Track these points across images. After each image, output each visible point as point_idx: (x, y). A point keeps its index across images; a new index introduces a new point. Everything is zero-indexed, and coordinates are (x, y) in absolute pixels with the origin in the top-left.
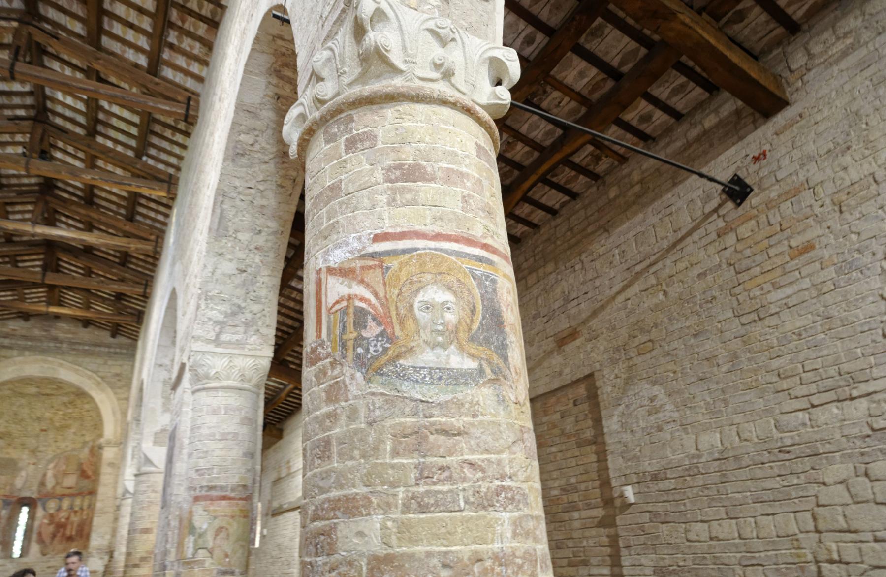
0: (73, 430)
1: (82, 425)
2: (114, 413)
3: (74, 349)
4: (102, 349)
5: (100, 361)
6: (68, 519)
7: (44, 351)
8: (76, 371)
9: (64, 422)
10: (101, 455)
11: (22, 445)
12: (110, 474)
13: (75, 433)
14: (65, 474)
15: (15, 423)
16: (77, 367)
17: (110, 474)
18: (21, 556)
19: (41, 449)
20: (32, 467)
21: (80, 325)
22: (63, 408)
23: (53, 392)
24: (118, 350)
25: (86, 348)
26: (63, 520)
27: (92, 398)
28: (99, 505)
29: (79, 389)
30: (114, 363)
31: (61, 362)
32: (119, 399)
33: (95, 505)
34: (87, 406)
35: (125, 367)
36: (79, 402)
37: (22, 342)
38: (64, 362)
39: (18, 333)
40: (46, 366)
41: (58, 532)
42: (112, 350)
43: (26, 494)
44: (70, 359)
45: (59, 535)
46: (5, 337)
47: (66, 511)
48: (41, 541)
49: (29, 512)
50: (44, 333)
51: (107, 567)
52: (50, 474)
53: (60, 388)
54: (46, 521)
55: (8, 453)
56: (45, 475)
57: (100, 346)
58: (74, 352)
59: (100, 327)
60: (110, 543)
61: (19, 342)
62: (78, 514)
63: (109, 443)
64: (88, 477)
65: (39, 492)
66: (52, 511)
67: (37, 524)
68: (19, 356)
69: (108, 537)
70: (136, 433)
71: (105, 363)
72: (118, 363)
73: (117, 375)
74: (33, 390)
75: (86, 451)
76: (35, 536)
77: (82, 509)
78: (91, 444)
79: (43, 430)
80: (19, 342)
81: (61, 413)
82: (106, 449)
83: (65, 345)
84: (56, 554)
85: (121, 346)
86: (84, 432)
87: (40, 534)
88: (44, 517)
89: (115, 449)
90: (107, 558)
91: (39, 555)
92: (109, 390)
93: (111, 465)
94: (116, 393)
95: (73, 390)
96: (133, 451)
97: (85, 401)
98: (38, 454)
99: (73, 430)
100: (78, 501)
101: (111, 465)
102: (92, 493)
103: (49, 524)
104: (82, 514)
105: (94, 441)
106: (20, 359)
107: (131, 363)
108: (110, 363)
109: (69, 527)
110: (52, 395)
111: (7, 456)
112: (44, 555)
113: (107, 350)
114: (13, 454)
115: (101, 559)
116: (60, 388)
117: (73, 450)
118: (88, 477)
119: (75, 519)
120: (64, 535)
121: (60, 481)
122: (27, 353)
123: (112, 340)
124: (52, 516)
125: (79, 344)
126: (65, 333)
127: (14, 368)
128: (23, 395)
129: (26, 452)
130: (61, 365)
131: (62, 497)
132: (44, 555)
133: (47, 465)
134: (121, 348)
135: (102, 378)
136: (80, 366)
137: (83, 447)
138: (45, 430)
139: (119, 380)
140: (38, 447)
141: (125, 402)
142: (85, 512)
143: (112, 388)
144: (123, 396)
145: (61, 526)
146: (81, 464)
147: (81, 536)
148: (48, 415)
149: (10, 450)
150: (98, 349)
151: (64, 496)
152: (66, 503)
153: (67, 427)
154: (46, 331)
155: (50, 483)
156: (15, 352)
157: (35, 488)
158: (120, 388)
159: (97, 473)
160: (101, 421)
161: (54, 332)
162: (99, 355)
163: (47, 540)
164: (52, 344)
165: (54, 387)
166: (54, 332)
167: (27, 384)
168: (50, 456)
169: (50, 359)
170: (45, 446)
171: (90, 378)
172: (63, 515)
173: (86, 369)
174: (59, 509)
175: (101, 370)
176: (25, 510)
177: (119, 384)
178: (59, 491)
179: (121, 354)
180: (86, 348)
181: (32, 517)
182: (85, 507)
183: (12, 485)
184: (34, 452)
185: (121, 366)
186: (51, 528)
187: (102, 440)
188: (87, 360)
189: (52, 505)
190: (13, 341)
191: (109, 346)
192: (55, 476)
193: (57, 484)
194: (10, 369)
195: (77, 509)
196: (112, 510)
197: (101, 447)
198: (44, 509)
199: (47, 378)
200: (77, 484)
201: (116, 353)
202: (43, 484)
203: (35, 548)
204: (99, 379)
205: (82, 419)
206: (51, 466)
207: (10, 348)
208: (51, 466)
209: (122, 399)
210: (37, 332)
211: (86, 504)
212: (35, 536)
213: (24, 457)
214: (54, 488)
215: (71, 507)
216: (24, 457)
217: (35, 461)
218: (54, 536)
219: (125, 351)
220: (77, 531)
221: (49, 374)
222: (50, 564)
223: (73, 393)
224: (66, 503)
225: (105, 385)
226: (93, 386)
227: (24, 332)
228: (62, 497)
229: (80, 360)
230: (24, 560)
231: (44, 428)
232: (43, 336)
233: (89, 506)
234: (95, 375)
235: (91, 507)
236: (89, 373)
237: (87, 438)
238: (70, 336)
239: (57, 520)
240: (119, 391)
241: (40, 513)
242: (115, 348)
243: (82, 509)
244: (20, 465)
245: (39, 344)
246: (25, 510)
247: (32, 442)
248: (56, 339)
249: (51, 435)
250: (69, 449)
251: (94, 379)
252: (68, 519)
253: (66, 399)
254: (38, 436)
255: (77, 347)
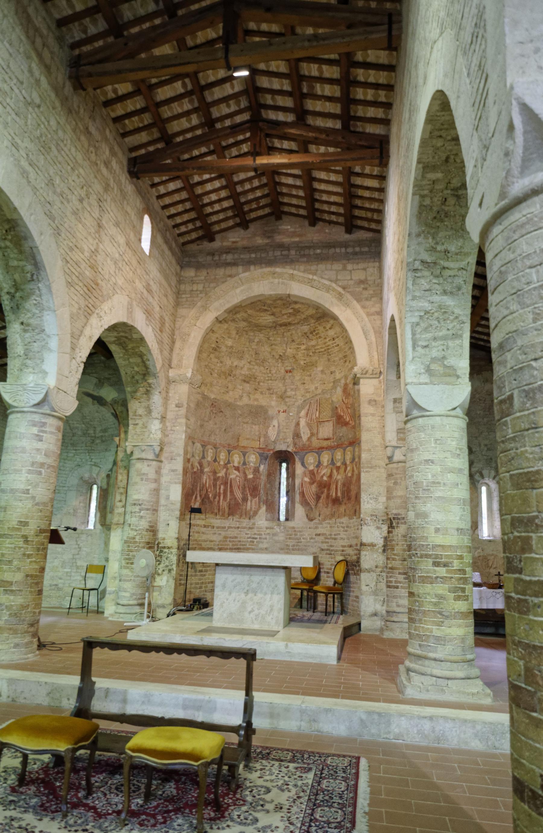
0: (320, 368)
1: (329, 360)
2: (365, 333)
3: (304, 256)
4: (338, 250)
5: (337, 266)
6: (330, 476)
7: (270, 263)
8: (310, 283)
9: (308, 360)
10: (359, 391)
11: (269, 389)
12: (373, 415)
13: (322, 372)
14: (320, 422)
15: (257, 364)
16: (311, 276)
17: (373, 415)
18: (287, 519)
19: (289, 393)
20: (282, 416)
21: (306, 223)
22: (305, 341)
23: (290, 320)
24: (357, 249)
25: (318, 251)
26: (325, 478)
27: (335, 318)
28: (364, 456)
29: (317, 307)
30: (355, 266)
31: (291, 272)
32: (368, 314)
33: (360, 457)
34: (331, 333)
35: (370, 270)
36: (321, 328)
37: (245, 256)
38: (295, 272)
39: (240, 244)
40: (276, 281)
41: (322, 493)
42: (350, 250)
43: (283, 447)
44: (302, 268)
45: (324, 496)
46: (227, 253)
47: (327, 467)
48: (305, 503)
49: (287, 469)
50: (266, 241)
51: (386, 538)
52: (303, 422)
53: (297, 312)
54: (307, 479)
55: (256, 400)
56: (298, 424)
57: (334, 247)
58: (305, 259)
59: (330, 222)
60: (386, 508)
61: (242, 256)
62: (342, 470)
63: (365, 372)
64: (346, 424)
65: (295, 444)
66: (311, 468)
67: (298, 482)
68: (244, 272)
69: (383, 499)
70: (414, 298)
71: (345, 268)
72: (361, 266)
73: (361, 282)
74: (267, 319)
75: (339, 390)
76: (298, 497)
77: (344, 463)
78: (343, 381)
79: (287, 372)
80: (242, 256)
81: (303, 347)
82: (362, 381)
83: (293, 252)
84: (324, 520)
85: (360, 243)
86: (333, 369)
87: (302, 494)
88: (305, 474)
89: (375, 382)
90: (385, 528)
91: (306, 520)
92: (355, 302)
93: (371, 402)
94: (363, 307)
95: (311, 311)
96: (414, 334)
97: (328, 326)
98: (287, 400)
99: (320, 368)
100: (339, 455)
101: (371, 402)
102: (355, 442)
103: (312, 482)
104: (345, 471)
105: (346, 377)
106: (247, 274)
107: (377, 264)
108: (350, 267)
109: (333, 487)
110: (290, 324)
111: (256, 403)
112: (311, 520)
113: (343, 250)
114: (263, 401)
115: (378, 528)
116: (297, 312)
117: (324, 392)
118: (346, 424)
119: (339, 477)
120: (328, 496)
121: (315, 431)
122: (252, 267)
123: (347, 236)
124: (312, 473)
125: (309, 248)
126: (292, 237)
127: (242, 288)
128: (259, 328)
129: (274, 397)
130: (292, 277)
131: (320, 450)
132: (311, 520)
133: (299, 412)
134: (359, 246)
135: (344, 288)
136: (315, 274)
137: (334, 388)
138: (290, 371)
139: (365, 289)
140: (285, 391)
141: (376, 317)
142: (349, 468)
143: (359, 300)
144: (373, 310)
145: (324, 486)
146: (336, 408)
147: (349, 499)
148: (290, 352)
149: (258, 396)
150: (332, 251)
151: (322, 448)
152: (325, 458)
153: (313, 365)
154: (269, 237)
155: (305, 434)
156: (240, 269)
157: (290, 440)
158: (367, 299)
159: (356, 416)
160: (351, 348)
161: (279, 238)
162: (335, 258)
163: (312, 503)
164: (278, 253)
165: (291, 311)
166: (279, 238)
167: (260, 310)
168: (300, 402)
169: (278, 270)
170: (292, 390)
171: (328, 289)
172: (325, 471)
173: (322, 278)
174: (319, 465)
175: (339, 277)
176: (284, 465)
177: (366, 294)
178: (315, 443)
179: (362, 253)
180: (318, 251)
181: (291, 475)
182: (348, 463)
183: (266, 436)
184: (282, 397)
185: (365, 269)
186: (314, 488)
187: (356, 369)
188: (322, 266)
189: (311, 459)
190: (236, 256)
191: (345, 245)
192: (309, 425)
193: (312, 434)
194: (238, 291)
195: (339, 464)
196: (382, 463)
197: (356, 381)
198: (303, 464)
199: (280, 298)
200: (334, 433)
201: (355, 254)
202: (297, 435)
203: (300, 511)
204: (340, 290)
205: (327, 351)
206: (303, 413)
207: (234, 264)
208: (303, 413)
209: (372, 314)
210: (260, 241)
211: (348, 457)
212: (298, 497)
213: (273, 403)
214: (309, 439)
215: (333, 462)
216: (273, 403)
217: (285, 408)
218: (318, 498)
219: (366, 249)
220: (343, 493)
221: (281, 291)
222: (318, 531)
223: (312, 316)
224: (325, 458)
225: (348, 296)
226: (335, 301)
227: (245, 243)
228: (320, 450)
229: (314, 268)
230: (290, 524)
231: (289, 368)
232: (267, 244)
233: (353, 460)
234: (334, 285)
235: (356, 460)
236: (327, 283)
237: (338, 376)
238: (297, 239)
239: (318, 478)
240: (368, 303)
241: (299, 469)
242: (354, 247)
243: (344, 463)
244: (270, 412)
245: (263, 255)
246: (284, 465)
247: (278, 386)
248: (281, 246)
249: (297, 376)
250: (319, 391)
251: (334, 290)
252: (330, 476)
253: (306, 328)
254: (284, 379)
255: (307, 252)
